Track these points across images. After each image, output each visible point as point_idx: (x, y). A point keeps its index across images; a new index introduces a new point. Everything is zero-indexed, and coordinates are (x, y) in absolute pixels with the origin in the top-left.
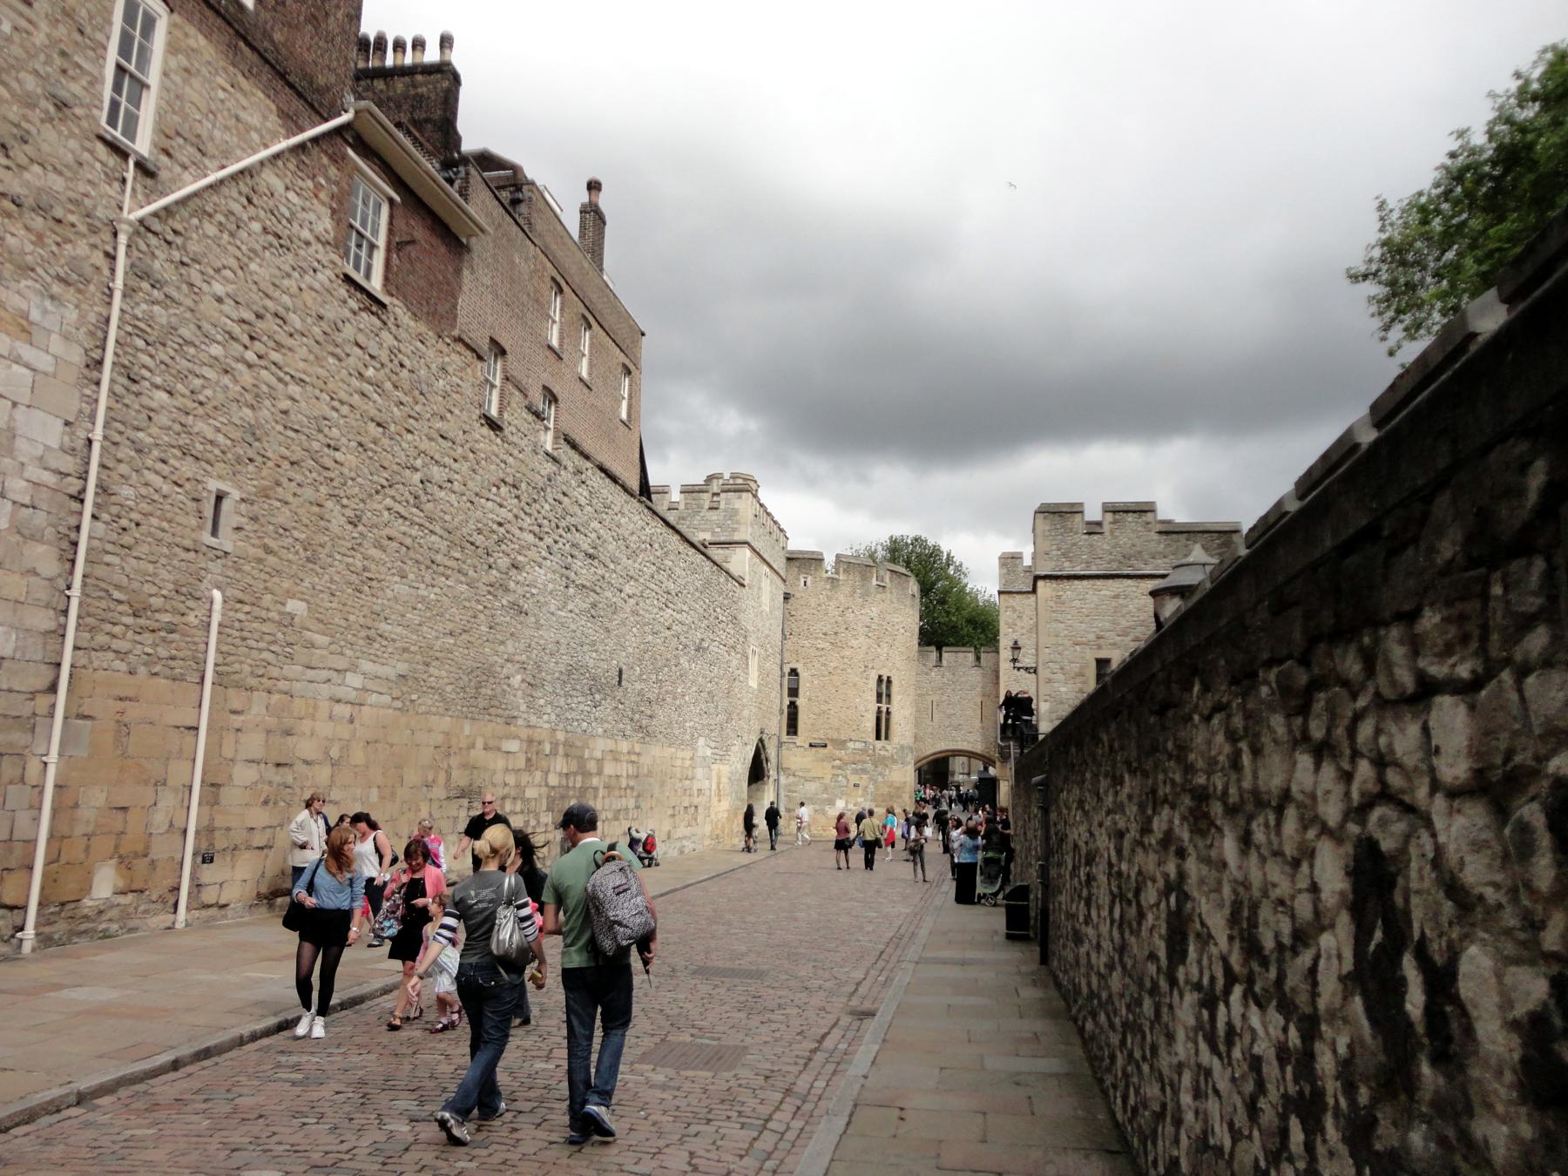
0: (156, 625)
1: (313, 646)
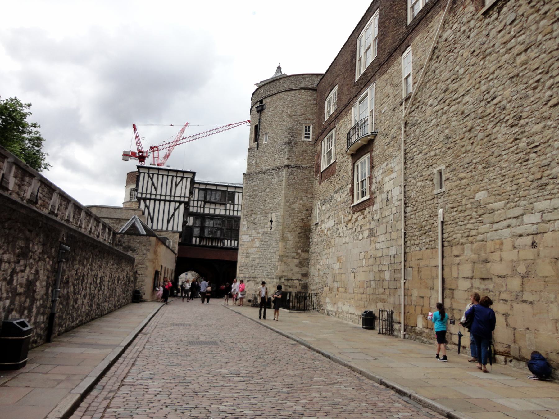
0: (424, 232)
1: (494, 211)
